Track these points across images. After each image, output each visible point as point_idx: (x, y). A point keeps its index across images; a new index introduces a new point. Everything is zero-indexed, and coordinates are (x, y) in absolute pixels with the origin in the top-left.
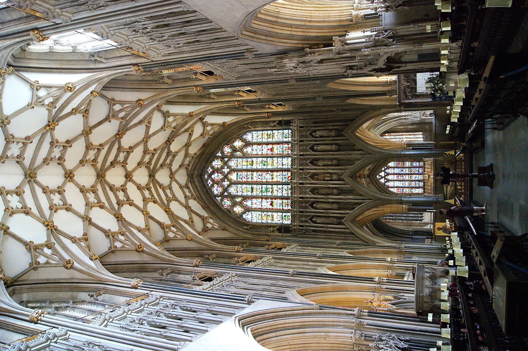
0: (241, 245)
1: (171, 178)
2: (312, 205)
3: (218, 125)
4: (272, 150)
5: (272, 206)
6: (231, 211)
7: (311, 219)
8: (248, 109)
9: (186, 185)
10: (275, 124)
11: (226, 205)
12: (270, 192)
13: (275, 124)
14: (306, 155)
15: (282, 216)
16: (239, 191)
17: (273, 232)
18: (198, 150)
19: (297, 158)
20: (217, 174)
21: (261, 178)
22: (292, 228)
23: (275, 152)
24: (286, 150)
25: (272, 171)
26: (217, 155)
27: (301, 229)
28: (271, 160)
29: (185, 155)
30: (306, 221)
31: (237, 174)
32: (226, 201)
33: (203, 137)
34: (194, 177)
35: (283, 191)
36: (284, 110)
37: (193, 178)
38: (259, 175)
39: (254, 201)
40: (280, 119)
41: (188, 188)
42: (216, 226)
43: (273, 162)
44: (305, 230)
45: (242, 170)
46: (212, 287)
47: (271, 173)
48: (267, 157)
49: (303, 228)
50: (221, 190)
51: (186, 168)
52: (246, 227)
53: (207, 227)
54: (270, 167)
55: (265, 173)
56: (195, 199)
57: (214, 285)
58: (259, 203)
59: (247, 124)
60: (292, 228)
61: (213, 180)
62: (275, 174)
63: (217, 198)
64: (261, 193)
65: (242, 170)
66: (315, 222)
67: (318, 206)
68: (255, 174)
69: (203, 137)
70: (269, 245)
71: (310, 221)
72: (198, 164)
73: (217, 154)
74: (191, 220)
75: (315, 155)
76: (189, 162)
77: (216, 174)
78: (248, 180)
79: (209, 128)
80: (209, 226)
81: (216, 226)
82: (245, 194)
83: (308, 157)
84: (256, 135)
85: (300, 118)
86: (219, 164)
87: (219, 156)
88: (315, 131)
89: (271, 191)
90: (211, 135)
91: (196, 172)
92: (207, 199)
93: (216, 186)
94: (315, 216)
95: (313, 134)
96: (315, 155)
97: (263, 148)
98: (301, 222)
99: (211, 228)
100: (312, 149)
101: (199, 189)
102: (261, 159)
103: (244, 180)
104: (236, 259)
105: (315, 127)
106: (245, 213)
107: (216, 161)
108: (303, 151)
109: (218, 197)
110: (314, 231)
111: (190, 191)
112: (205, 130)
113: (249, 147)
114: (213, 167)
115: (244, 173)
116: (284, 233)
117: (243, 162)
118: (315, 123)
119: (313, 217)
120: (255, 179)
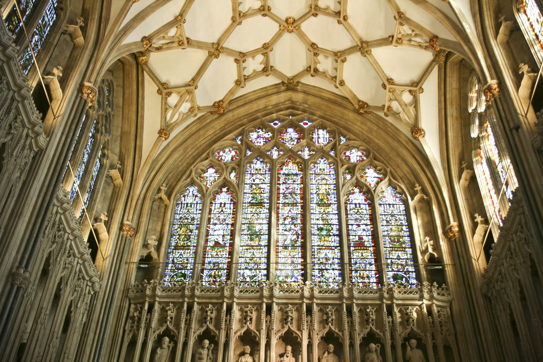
0: (119, 166)
1: (287, 21)
2: (207, 335)
3: (417, 118)
4: (360, 245)
5: (213, 248)
6: (206, 162)
7: (167, 333)
8: (462, 180)
9: (272, 67)
10: (430, 250)
11: (221, 153)
12: (249, 242)
13: (430, 250)
14: (351, 324)
15: (185, 268)
16: (254, 177)
17: (145, 245)
18: (351, 92)
19: (341, 298)
20: (297, 136)
21: (287, 222)
22: (149, 283)
23: (356, 255)
24: (363, 278)
25: (304, 246)
26: (342, 138)
27: (142, 308)
28: (332, 244)
29: (339, 52)
30: (163, 320)
31: (296, 175)
32: (233, 153)
33: (386, 83)
34: (289, 94)
35: (251, 269)
36: (474, 261)
37: (288, 89)
38: (293, 219)
39: (229, 208)
40: (446, 259)
41: (265, 70)
42: (172, 116)
43: (329, 248)
44: (140, 319)
45: (304, 181)
46: (87, 278)
47: (299, 244)
48: (340, 235)
49: (145, 313)
50: (259, 144)
51: (310, 67)
52: (164, 188)
53: (169, 94)
54: (315, 241)
55: (300, 232)
56: (238, 83)
57: (84, 261)
58: (222, 217)
59: (424, 191)
60: (149, 283)
61: (282, 131)
62: (298, 253)
63: (240, 138)
64: (247, 221)
65: (304, 181)
66: (159, 342)
67: (205, 352)
68: (298, 210)
69: (386, 83)
70: (108, 225)
71: (162, 329)
72: (317, 100)
73: (344, 137)
74: (185, 42)
75: (352, 345)
76: (324, 73)
77: (295, 135)
78: (282, 195)
79: (407, 98)
80: (173, 100)
81: (172, 116)
82: (247, 189)
83: (346, 327)
84: (395, 212)
85: (455, 307)
86: (321, 140)
87: (340, 140)
88: (421, 346)
89: (252, 243)
90: (389, 107)
91: (298, 97)
92: (240, 119)
93: (269, 135)
94: (176, 343)
95: (414, 342)
96: (352, 345)
97: (363, 227)
98: (164, 311)
99: (166, 103)
100: (370, 338)
101: (261, 104)
102: (335, 222)
103: (282, 187)
104: (104, 217)
105: (435, 347)
106: (200, 190)
107: (327, 136)
108: (361, 317)
109: (241, 140)
110: (133, 343)
111: (256, 74)
112: (402, 88)
113: (363, 197)
114: (312, 130)
115: (298, 188)
116: (139, 268)
117: (327, 187)
118: (447, 348)
119: (174, 339)
120: (285, 211)
